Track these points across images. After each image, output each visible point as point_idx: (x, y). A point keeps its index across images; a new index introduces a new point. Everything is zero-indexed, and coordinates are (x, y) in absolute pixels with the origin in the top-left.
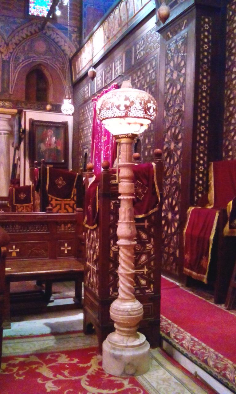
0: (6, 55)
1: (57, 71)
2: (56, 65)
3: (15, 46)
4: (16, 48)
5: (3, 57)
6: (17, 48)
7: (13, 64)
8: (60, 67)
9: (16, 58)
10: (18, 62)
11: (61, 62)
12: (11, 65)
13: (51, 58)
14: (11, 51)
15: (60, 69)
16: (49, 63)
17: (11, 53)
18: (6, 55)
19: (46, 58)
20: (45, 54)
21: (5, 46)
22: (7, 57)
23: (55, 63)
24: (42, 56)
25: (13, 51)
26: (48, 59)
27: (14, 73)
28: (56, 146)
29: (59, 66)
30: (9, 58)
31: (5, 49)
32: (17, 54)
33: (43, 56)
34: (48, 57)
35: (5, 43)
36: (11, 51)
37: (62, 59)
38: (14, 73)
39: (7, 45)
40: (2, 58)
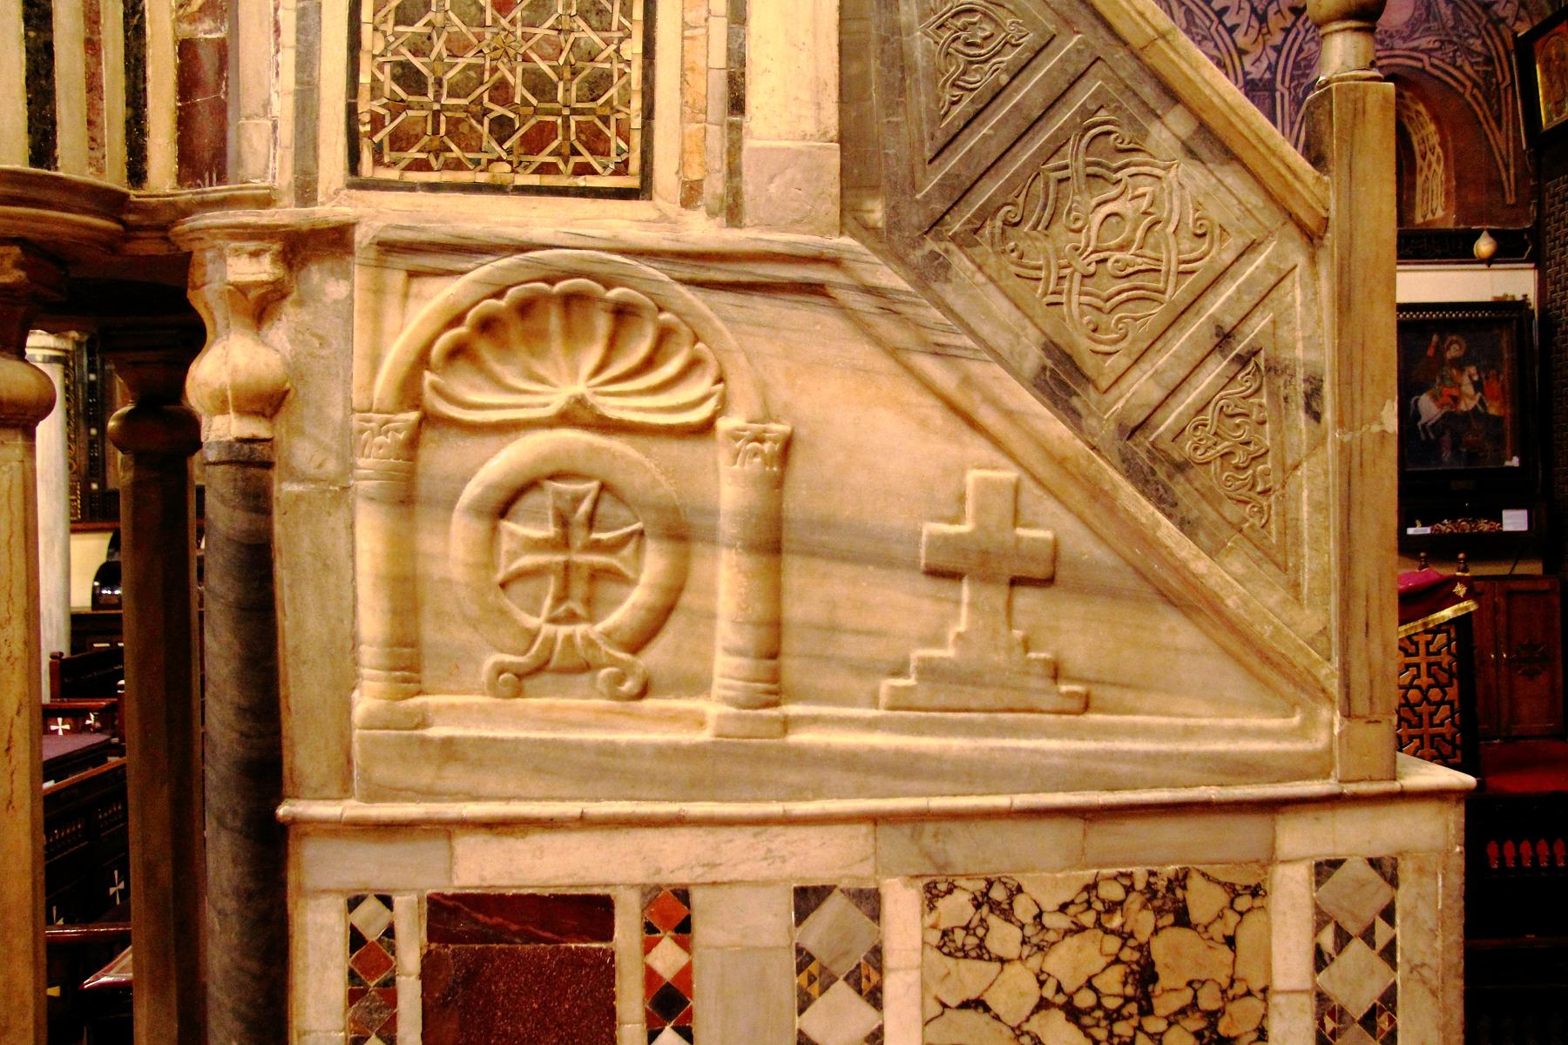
0: (1258, 59)
1: (1462, 96)
2: (1460, 69)
3: (1290, 18)
4: (1294, 25)
5: (1248, 68)
6: (1299, 23)
7: (1287, 93)
8: (1474, 75)
9: (1296, 65)
10: (1306, 82)
11: (1479, 54)
12: (1278, 95)
13: (1437, 45)
14: (1277, 38)
15: (1475, 85)
16: (1428, 68)
17: (1278, 49)
18: (1258, 59)
19: (1414, 49)
20: (1413, 32)
21: (1255, 23)
22: (1265, 64)
23: (1454, 65)
24: (1398, 43)
25: (1285, 40)
26: (1428, 52)
27: (1292, 124)
28: (1481, 401)
29: (1468, 68)
30: (1272, 68)
31: (1253, 34)
32: (1300, 50)
33: (1405, 40)
34: (1424, 43)
35: (1254, 10)
36: (1277, 38)
37: (1484, 44)
38: (1292, 124)
39: (1263, 19)
40: (1245, 74)
